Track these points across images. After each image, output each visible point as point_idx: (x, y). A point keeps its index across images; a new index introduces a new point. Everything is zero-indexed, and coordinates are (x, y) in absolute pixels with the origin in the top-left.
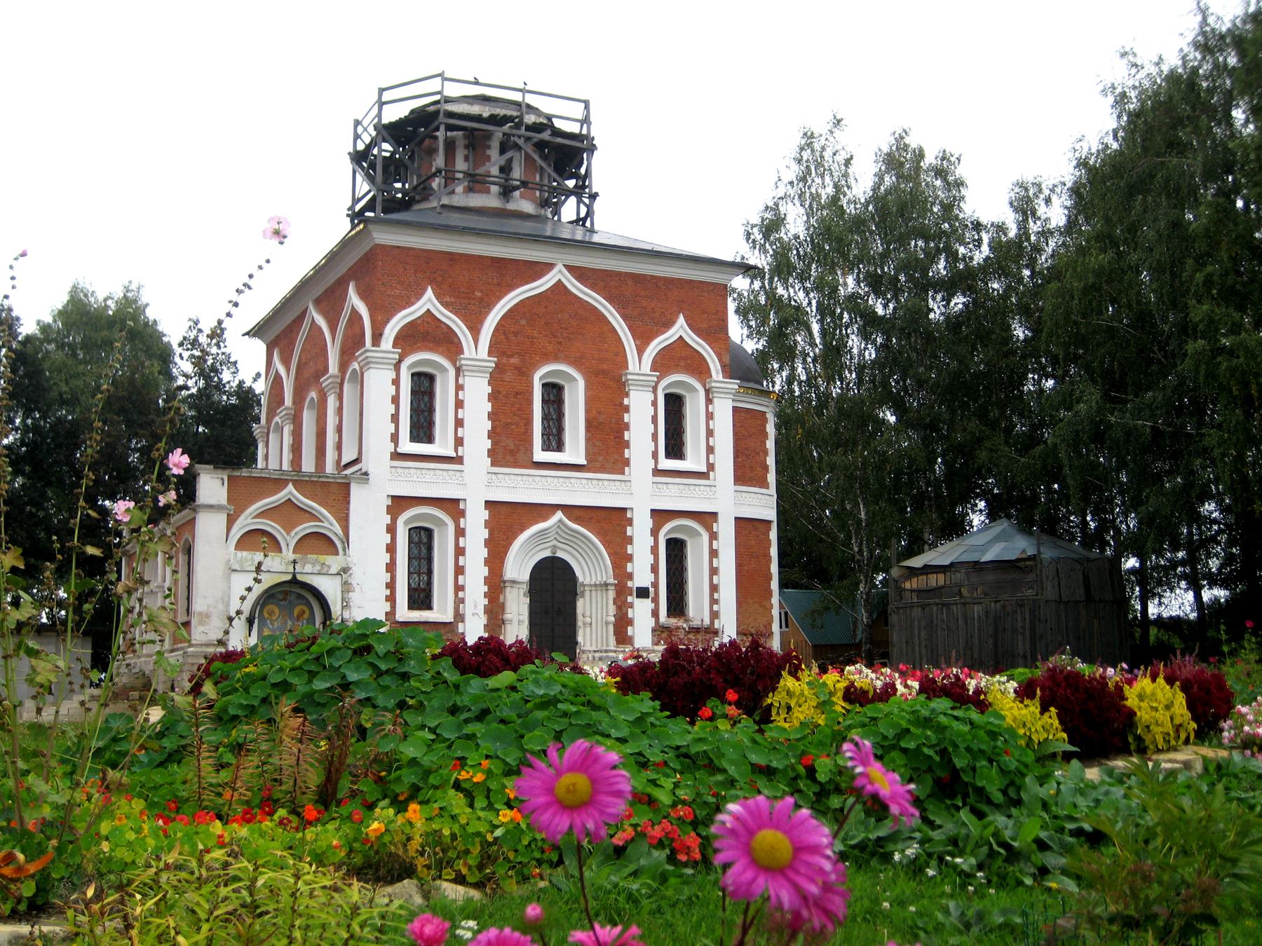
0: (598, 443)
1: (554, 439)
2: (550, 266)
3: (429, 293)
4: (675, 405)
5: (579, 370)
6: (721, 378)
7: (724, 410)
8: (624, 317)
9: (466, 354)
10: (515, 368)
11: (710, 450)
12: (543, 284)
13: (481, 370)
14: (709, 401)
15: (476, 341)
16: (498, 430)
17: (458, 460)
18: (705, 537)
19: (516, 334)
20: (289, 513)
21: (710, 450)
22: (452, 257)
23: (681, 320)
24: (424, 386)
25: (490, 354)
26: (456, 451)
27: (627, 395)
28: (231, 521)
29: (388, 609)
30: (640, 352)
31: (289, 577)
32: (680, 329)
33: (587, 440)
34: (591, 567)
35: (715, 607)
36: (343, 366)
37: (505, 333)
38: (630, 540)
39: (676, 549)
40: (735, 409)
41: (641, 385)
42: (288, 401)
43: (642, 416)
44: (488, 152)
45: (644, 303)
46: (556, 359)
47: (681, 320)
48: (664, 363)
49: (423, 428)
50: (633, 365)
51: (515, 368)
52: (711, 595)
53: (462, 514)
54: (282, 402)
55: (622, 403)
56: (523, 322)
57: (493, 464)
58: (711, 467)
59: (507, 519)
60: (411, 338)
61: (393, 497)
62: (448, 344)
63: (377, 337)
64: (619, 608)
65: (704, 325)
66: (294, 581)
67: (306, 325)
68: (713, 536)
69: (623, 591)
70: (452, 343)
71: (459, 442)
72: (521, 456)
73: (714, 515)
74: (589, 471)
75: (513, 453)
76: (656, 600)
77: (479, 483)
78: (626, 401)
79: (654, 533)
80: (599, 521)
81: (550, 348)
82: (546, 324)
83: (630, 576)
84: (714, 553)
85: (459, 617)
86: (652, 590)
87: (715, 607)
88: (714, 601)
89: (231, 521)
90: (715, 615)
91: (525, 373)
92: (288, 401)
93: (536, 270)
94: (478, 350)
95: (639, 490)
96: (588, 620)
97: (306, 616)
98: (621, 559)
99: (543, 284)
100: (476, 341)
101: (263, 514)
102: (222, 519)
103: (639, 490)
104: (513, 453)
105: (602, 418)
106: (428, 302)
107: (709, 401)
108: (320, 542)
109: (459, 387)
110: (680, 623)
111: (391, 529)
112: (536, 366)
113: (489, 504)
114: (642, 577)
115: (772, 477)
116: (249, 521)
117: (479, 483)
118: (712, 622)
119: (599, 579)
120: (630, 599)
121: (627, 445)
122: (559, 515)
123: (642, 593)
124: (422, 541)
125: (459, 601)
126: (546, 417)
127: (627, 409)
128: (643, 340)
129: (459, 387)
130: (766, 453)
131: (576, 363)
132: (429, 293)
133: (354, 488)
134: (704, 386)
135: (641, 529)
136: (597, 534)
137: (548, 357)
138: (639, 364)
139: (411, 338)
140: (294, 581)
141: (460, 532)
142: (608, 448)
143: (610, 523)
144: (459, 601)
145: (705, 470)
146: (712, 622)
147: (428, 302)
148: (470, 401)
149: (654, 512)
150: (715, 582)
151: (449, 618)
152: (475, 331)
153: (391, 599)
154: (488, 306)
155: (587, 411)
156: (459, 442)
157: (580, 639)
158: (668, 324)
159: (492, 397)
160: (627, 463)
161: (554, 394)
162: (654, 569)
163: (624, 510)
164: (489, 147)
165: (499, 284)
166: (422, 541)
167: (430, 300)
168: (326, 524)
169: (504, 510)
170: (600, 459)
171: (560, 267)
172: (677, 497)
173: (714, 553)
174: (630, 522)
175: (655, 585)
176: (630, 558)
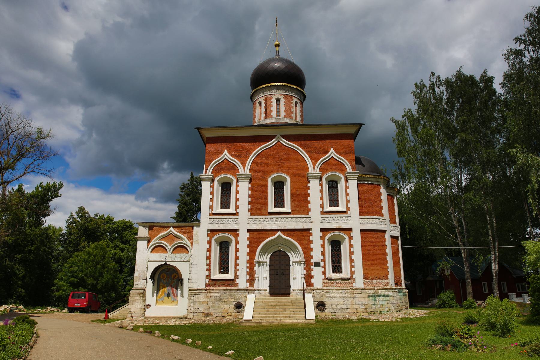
0: (297, 203)
1: (279, 203)
2: (276, 136)
3: (226, 152)
5: (288, 174)
6: (351, 171)
7: (353, 184)
8: (307, 152)
9: (241, 173)
10: (261, 176)
11: (348, 201)
13: (245, 178)
14: (347, 181)
15: (244, 168)
16: (253, 201)
18: (347, 239)
19: (261, 163)
20: (171, 237)
21: (348, 201)
24: (226, 187)
25: (250, 172)
26: (236, 210)
27: (309, 182)
28: (149, 241)
29: (208, 274)
30: (314, 165)
31: (164, 263)
32: (332, 153)
33: (292, 202)
35: (353, 269)
37: (256, 164)
38: (311, 242)
39: (336, 245)
40: (358, 183)
41: (314, 178)
43: (316, 190)
44: (272, 104)
45: (316, 145)
46: (278, 171)
48: (325, 168)
49: (225, 204)
50: (311, 170)
51: (261, 176)
52: (351, 264)
53: (238, 235)
55: (307, 186)
56: (264, 159)
57: (251, 215)
58: (348, 209)
59: (256, 236)
60: (219, 169)
61: (211, 231)
62: (233, 169)
63: (206, 170)
64: (307, 271)
65: (343, 151)
66: (166, 264)
68: (351, 238)
69: (308, 263)
70: (235, 169)
71: (237, 207)
72: (263, 211)
73: (350, 229)
74: (293, 214)
75: (260, 210)
76: (324, 267)
77: (244, 222)
78: (309, 185)
79: (322, 238)
80: (297, 235)
81: (275, 167)
82: (274, 158)
83: (312, 257)
84: (351, 246)
85: (236, 277)
86: (322, 264)
87: (353, 269)
88: (352, 267)
90: (353, 273)
94: (244, 170)
95: (315, 221)
96: (295, 276)
97: (176, 277)
98: (307, 250)
100: (244, 168)
103: (315, 221)
104: (260, 210)
105: (298, 193)
106: (226, 155)
107: (347, 181)
108: (182, 248)
109: (237, 186)
110: (338, 276)
111: (209, 243)
112: (269, 175)
113: (249, 231)
114: (316, 256)
115: (385, 211)
116: (157, 242)
117: (244, 222)
118: (352, 276)
119: (298, 259)
120: (312, 267)
121: (309, 202)
122: (279, 233)
123: (317, 264)
124: (224, 246)
125: (236, 270)
128: (315, 159)
129: (237, 186)
130: (381, 201)
131: (287, 172)
132: (226, 152)
133: (195, 228)
134: (344, 175)
135: (316, 238)
136: (296, 240)
137: (274, 171)
138: (313, 169)
139: (219, 169)
140: (166, 264)
141: (237, 243)
142: (301, 204)
144: (236, 270)
145: (345, 210)
146: (352, 276)
148: (242, 192)
149: (322, 230)
150: (352, 258)
151: (233, 277)
152: (244, 164)
153: (209, 270)
154: (250, 154)
155: (291, 190)
156: (237, 207)
157: (292, 284)
158: (326, 153)
159: (250, 189)
160: (309, 210)
161: (279, 186)
162: (323, 253)
163: (309, 230)
164: (272, 102)
165: (254, 146)
166: (224, 246)
167: (225, 154)
168: (184, 242)
169: (255, 233)
170: (298, 209)
171: (278, 136)
173: (351, 246)
174: (311, 234)
175: (324, 261)
176: (311, 250)
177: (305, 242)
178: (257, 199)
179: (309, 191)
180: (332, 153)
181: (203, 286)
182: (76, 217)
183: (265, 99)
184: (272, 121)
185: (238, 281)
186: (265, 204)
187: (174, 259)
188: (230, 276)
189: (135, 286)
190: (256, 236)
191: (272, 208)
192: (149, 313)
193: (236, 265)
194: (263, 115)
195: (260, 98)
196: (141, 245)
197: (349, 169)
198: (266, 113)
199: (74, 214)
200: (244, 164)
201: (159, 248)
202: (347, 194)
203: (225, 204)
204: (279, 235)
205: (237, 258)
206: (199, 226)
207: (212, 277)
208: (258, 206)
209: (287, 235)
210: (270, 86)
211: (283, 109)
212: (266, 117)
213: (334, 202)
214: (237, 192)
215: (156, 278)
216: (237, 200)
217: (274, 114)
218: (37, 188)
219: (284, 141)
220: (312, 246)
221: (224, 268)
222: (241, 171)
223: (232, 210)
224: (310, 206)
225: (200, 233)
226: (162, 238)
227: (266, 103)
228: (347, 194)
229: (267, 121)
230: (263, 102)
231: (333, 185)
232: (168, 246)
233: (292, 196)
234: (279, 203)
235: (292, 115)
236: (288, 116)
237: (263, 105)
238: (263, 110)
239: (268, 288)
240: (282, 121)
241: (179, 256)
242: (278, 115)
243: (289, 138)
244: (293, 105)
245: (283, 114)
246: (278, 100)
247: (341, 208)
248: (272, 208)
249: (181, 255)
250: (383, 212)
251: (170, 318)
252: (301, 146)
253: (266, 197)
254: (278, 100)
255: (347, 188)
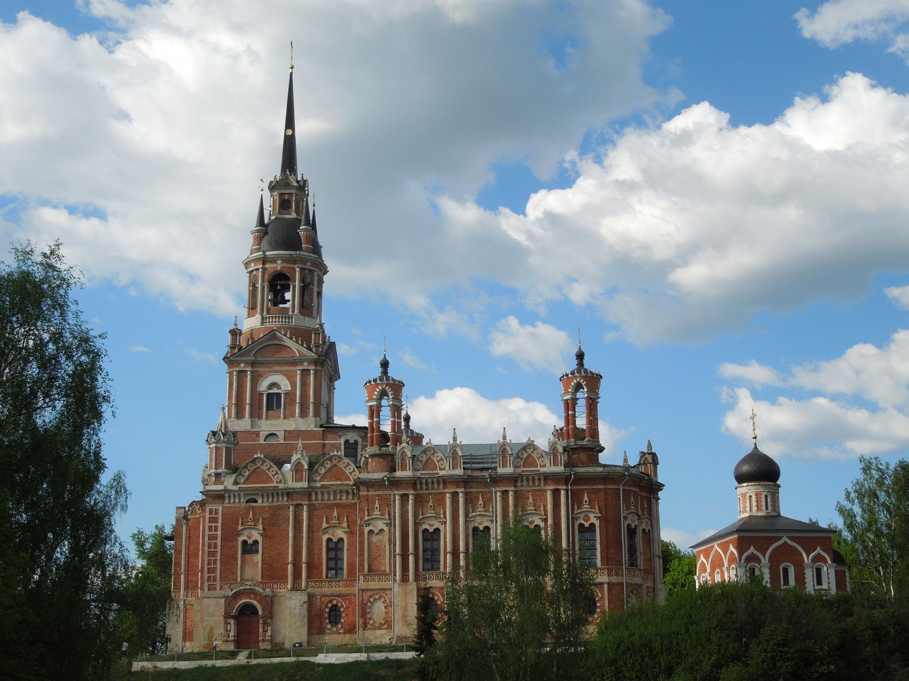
4: (819, 571)
12: (781, 542)
22: (758, 538)
32: (819, 550)
36: (729, 565)
42: (708, 570)
54: (705, 570)
62: (758, 560)
63: (740, 560)
67: (714, 551)
92: (708, 570)
93: (780, 538)
94: (765, 561)
99: (781, 542)
106: (752, 550)
126: (784, 577)
137: (783, 562)
147: (752, 550)
161: (786, 571)
180: (819, 550)
183: (756, 494)
184: (763, 514)
194: (754, 508)
197: (830, 562)
198: (757, 506)
212: (758, 510)
217: (764, 508)
238: (754, 504)
242: (767, 509)
254: (766, 496)
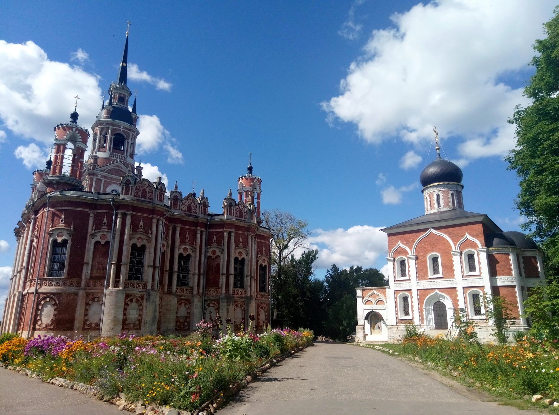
1: (436, 271)
5: (439, 253)
8: (450, 237)
11: (480, 268)
14: (478, 255)
17: (409, 280)
21: (480, 268)
23: (467, 234)
24: (403, 263)
28: (363, 298)
34: (448, 303)
38: (457, 296)
46: (433, 251)
47: (467, 234)
49: (403, 273)
50: (454, 249)
58: (481, 273)
59: (422, 292)
62: (405, 252)
71: (409, 276)
72: (425, 277)
73: (483, 286)
75: (424, 277)
77: (414, 284)
83: (459, 305)
89: (363, 298)
91: (424, 256)
94: (411, 253)
95: (459, 282)
98: (455, 301)
99: (426, 233)
101: (370, 296)
102: (361, 299)
103: (459, 282)
104: (424, 277)
109: (408, 263)
113: (418, 290)
117: (414, 284)
124: (405, 299)
127: (453, 261)
128: (455, 241)
135: (460, 292)
137: (430, 251)
141: (412, 297)
143: (452, 291)
148: (411, 265)
149: (464, 288)
154: (413, 242)
155: (442, 263)
156: (409, 276)
160: (454, 275)
161: (435, 260)
163: (456, 288)
172: (470, 283)
176: (458, 301)
177: (454, 296)
178: (421, 270)
179: (454, 263)
181: (395, 324)
182: (331, 272)
183: (430, 196)
185: (414, 320)
186: (426, 273)
187: (377, 308)
188: (410, 317)
189: (359, 324)
190: (422, 292)
191: (430, 274)
192: (368, 338)
193: (413, 311)
194: (429, 207)
195: (426, 193)
196: (359, 301)
197: (480, 246)
199: (330, 270)
200: (411, 248)
201: (368, 302)
202: (479, 263)
203: (403, 273)
204: (436, 293)
205: (412, 307)
206: (390, 288)
207: (400, 318)
208: (421, 274)
209: (442, 292)
210: (431, 186)
211: (442, 201)
213: (472, 267)
214: (409, 267)
215: (369, 319)
216: (409, 271)
217: (436, 205)
218: (302, 255)
219: (433, 231)
220: (458, 298)
221: (407, 313)
222: (410, 254)
223: (407, 278)
224: (455, 273)
225: (390, 292)
226: (370, 296)
227: (430, 198)
228: (479, 263)
229: (432, 212)
230: (428, 198)
231: (471, 257)
232: (373, 301)
233: (443, 267)
234: (436, 271)
235: (450, 204)
236: (446, 205)
237: (428, 200)
238: (429, 203)
239: (434, 325)
240: (442, 210)
241: (380, 306)
243: (436, 228)
244: (450, 196)
245: (442, 204)
246: (438, 196)
247: (477, 272)
248: (430, 274)
249: (381, 305)
250: (513, 272)
251: (378, 342)
252: (446, 233)
253: (427, 268)
254: (438, 196)
255: (479, 259)
